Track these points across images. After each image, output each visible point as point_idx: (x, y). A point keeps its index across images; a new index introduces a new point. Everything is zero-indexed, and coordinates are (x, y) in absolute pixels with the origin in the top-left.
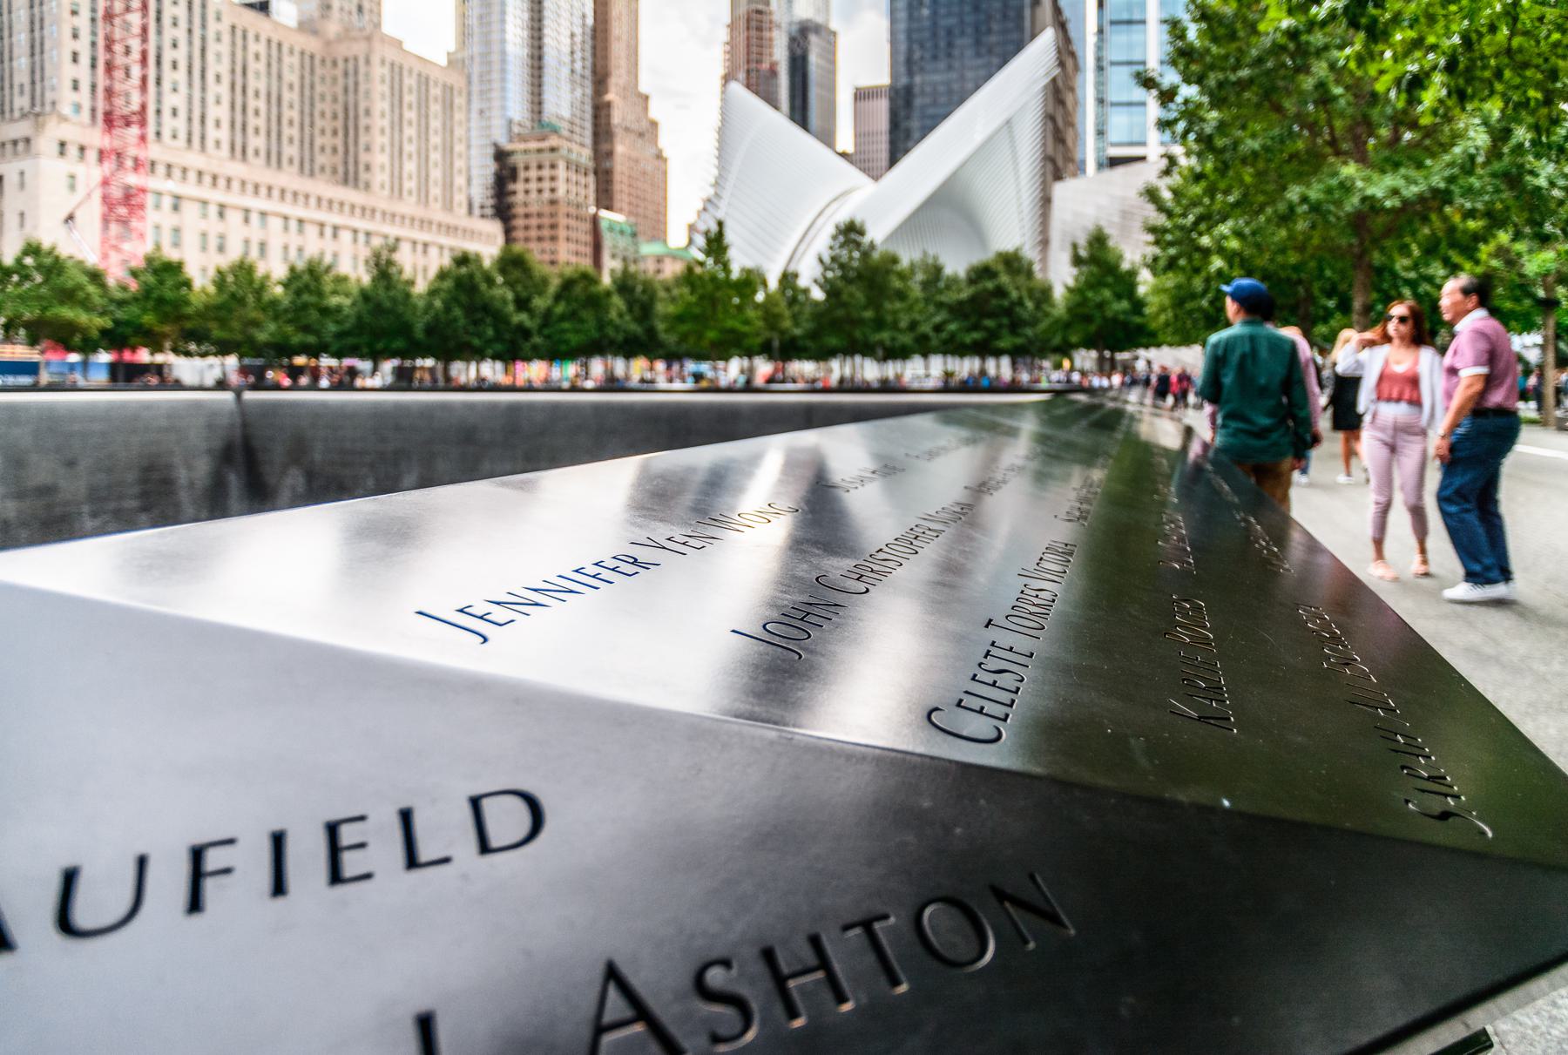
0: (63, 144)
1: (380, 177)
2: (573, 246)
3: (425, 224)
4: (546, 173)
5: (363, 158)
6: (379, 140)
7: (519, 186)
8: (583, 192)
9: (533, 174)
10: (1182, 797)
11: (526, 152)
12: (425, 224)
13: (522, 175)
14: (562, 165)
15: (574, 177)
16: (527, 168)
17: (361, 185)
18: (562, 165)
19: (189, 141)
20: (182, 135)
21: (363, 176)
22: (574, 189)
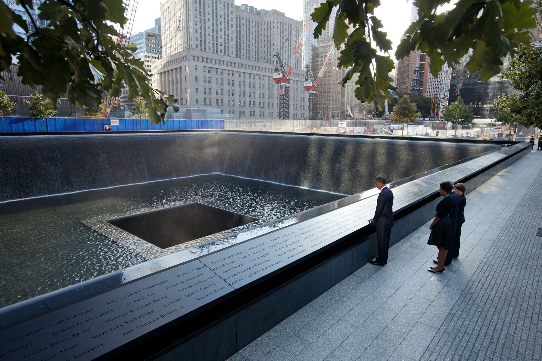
0: (194, 56)
7: (320, 59)
11: (323, 47)
13: (320, 55)
16: (322, 53)
17: (272, 62)
19: (225, 52)
20: (223, 51)
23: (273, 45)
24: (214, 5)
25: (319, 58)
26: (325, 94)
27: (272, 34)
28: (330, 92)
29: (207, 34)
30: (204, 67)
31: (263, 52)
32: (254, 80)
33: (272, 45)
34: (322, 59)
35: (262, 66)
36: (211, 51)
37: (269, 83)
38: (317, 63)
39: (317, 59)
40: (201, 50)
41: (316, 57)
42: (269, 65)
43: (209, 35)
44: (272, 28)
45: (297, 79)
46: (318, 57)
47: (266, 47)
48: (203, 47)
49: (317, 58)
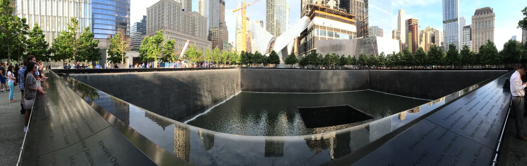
0: (166, 32)
4: (216, 34)
7: (212, 36)
13: (213, 34)
15: (220, 34)
21: (195, 35)
27: (195, 23)
29: (171, 21)
30: (171, 37)
31: (191, 31)
34: (217, 36)
36: (177, 31)
40: (168, 29)
42: (186, 35)
43: (172, 22)
44: (195, 20)
45: (206, 45)
46: (212, 35)
47: (192, 29)
48: (169, 28)
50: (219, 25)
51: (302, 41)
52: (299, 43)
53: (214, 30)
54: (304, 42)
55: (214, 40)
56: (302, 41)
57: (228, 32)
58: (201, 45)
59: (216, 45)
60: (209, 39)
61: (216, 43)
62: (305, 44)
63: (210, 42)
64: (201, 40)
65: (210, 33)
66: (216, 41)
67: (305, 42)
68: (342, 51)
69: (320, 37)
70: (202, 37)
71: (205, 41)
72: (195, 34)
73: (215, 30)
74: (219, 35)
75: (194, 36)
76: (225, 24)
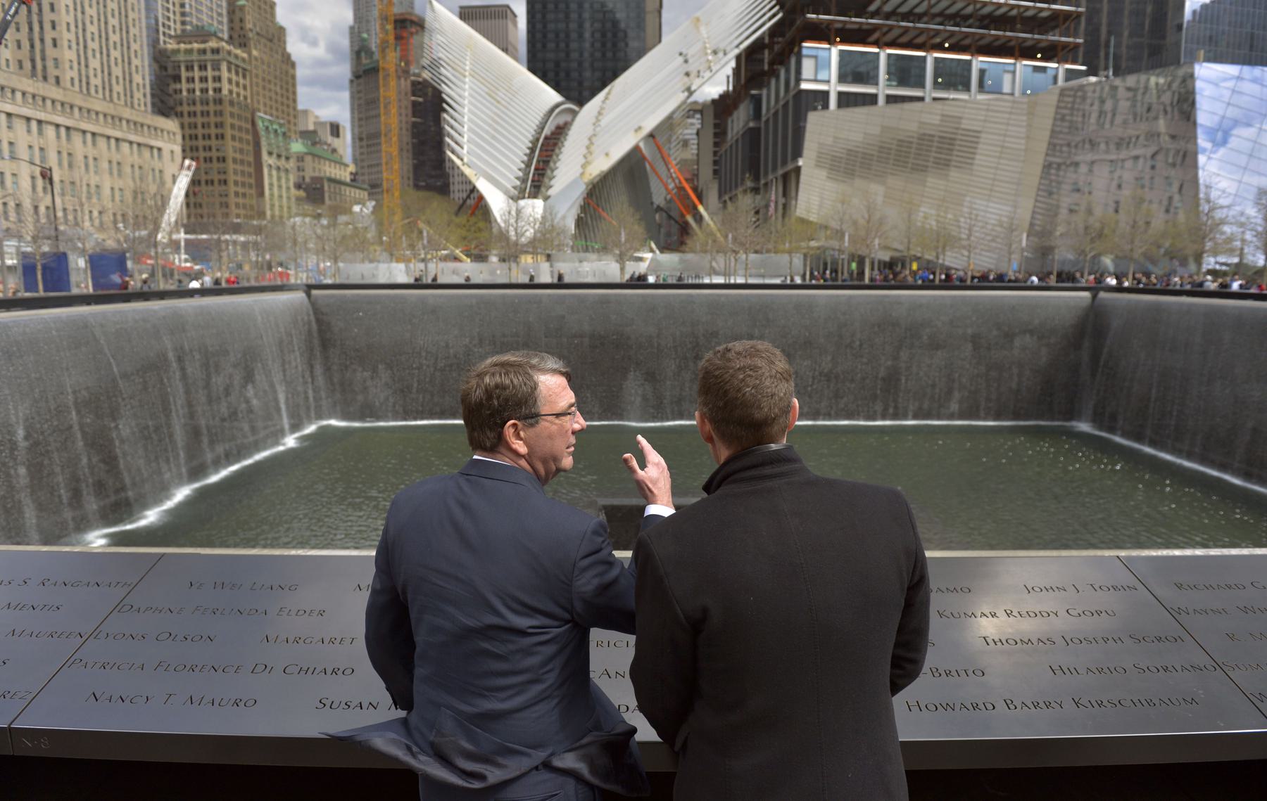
1: (69, 74)
2: (237, 144)
3: (116, 119)
5: (50, 52)
6: (66, 36)
8: (242, 92)
9: (197, 74)
10: (797, 405)
12: (116, 119)
13: (184, 74)
14: (224, 67)
15: (234, 78)
16: (189, 68)
18: (224, 67)
21: (52, 72)
22: (235, 89)
23: (54, 28)
24: (483, 81)
25: (180, 81)
26: (210, 188)
28: (228, 182)
32: (11, 135)
33: (47, 26)
35: (30, 90)
37: (59, 147)
38: (178, 97)
39: (178, 86)
41: (171, 81)
46: (177, 78)
49: (175, 82)
50: (225, 20)
51: (739, 121)
52: (720, 133)
53: (189, 52)
54: (747, 123)
55: (199, 108)
56: (739, 121)
57: (293, 65)
58: (102, 143)
59: (214, 143)
60: (164, 103)
61: (213, 131)
62: (753, 137)
63: (171, 125)
64: (98, 106)
65: (163, 68)
66: (213, 119)
67: (751, 124)
68: (954, 174)
69: (840, 94)
70: (107, 87)
71: (127, 113)
72: (50, 64)
73: (196, 46)
74: (230, 81)
75: (45, 78)
76: (273, 15)
